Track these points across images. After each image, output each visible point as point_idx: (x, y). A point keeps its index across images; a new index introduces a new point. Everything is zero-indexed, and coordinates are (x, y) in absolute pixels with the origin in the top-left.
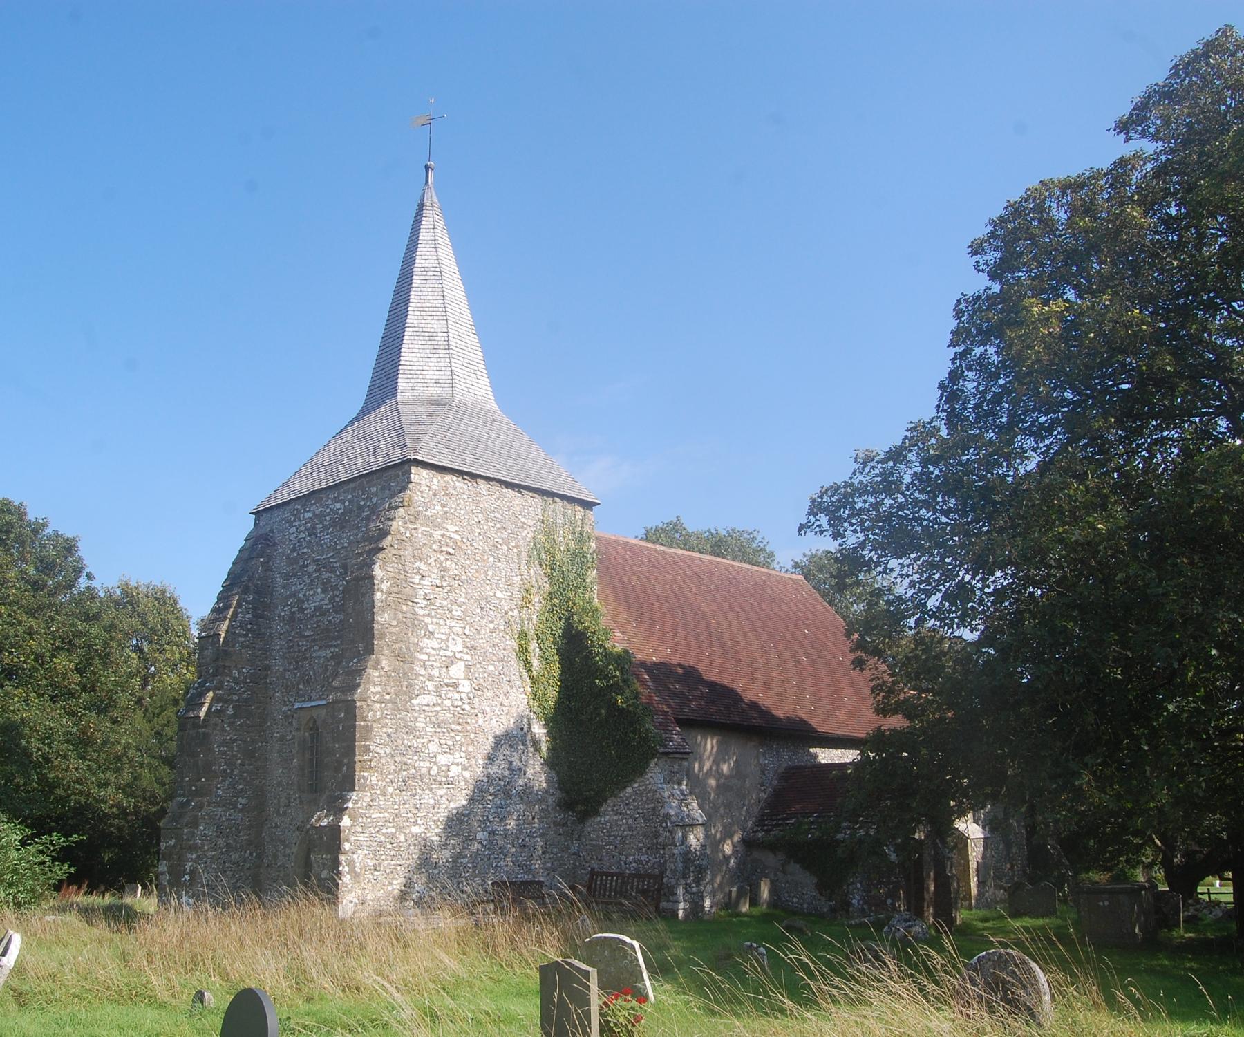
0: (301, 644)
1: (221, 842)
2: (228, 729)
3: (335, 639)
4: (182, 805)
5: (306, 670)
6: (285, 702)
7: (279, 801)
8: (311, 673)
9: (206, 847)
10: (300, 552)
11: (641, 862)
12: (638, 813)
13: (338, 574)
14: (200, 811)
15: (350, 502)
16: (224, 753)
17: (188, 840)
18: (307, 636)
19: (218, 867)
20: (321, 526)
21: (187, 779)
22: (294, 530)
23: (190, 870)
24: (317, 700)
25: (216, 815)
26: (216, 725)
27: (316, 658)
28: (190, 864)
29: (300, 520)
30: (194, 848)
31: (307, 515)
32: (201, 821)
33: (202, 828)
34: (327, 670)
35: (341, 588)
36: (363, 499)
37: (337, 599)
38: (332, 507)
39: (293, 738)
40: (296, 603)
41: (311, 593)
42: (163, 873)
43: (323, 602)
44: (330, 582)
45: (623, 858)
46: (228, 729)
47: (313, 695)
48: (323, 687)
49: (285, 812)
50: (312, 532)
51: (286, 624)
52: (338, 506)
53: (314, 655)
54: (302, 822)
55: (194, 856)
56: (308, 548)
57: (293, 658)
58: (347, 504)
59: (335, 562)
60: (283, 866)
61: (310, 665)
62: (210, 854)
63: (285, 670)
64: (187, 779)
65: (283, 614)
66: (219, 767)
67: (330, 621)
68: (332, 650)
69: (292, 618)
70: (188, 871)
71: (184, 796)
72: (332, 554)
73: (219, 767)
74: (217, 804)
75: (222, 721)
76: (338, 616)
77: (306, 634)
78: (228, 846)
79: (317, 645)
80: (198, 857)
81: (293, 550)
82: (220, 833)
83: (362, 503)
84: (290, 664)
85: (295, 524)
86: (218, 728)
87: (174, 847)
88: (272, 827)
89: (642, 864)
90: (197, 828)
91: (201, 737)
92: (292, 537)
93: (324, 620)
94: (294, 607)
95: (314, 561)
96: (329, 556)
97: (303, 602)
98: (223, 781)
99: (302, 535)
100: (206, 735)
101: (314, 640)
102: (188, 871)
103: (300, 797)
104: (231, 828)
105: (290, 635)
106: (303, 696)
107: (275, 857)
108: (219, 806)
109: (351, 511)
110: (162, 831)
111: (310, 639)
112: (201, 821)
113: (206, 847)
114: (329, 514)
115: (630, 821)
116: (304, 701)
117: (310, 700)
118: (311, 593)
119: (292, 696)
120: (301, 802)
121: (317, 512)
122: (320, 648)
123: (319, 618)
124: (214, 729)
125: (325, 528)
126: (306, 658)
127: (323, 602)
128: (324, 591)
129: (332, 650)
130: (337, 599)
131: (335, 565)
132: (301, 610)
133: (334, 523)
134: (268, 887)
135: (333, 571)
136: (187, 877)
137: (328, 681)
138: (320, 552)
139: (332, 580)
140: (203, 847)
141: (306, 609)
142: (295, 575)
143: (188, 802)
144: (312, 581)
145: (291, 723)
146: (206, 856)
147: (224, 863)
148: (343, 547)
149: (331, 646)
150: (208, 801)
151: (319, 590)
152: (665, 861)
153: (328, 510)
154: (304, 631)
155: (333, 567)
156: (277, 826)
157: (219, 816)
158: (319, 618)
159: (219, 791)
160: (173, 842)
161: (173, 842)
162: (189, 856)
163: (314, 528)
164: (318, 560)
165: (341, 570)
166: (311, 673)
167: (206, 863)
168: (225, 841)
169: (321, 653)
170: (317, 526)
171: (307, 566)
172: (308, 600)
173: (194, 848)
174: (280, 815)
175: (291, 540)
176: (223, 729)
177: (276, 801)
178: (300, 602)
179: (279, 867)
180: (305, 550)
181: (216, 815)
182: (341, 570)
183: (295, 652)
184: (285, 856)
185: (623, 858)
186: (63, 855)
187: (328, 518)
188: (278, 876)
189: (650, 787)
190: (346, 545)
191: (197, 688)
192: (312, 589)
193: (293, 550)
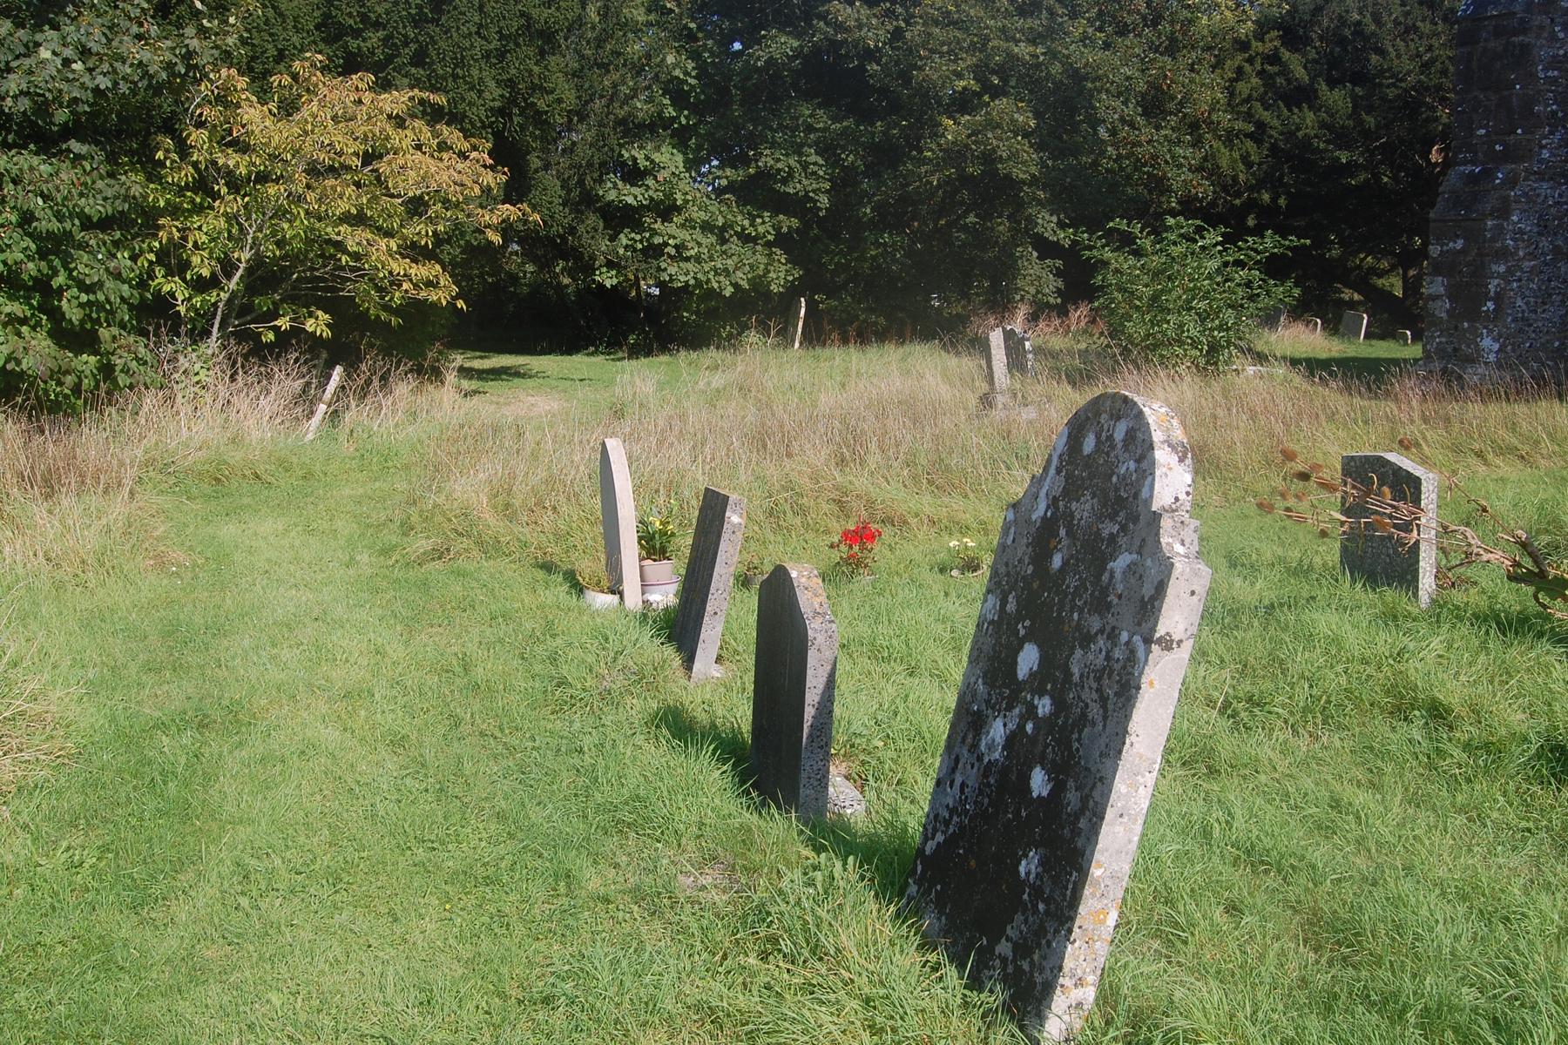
1: (1544, 243)
2: (1561, 35)
4: (1472, 179)
9: (1521, 253)
14: (1512, 189)
16: (1554, 80)
17: (1493, 240)
19: (1540, 289)
21: (1483, 132)
23: (1496, 292)
25: (1538, 195)
26: (1542, 28)
28: (1496, 282)
30: (1503, 254)
32: (1514, 206)
33: (1515, 218)
42: (1434, 298)
46: (1561, 35)
55: (1502, 269)
62: (1527, 265)
64: (1483, 132)
66: (1545, 108)
70: (1492, 294)
71: (1474, 162)
73: (1545, 108)
74: (1541, 176)
75: (1552, 20)
78: (1556, 250)
80: (1509, 271)
82: (1544, 228)
86: (1545, 35)
87: (1463, 251)
90: (1507, 219)
91: (1517, 52)
98: (1552, 133)
100: (1525, 49)
102: (1492, 294)
104: (1560, 219)
108: (1543, 180)
110: (1432, 225)
112: (1514, 206)
113: (1521, 253)
124: (1538, 37)
136: (1490, 305)
140: (1516, 253)
143: (1488, 174)
146: (1521, 270)
147: (1550, 280)
150: (1526, 170)
157: (1542, 198)
159: (1544, 151)
160: (1459, 244)
161: (1459, 244)
162: (1494, 267)
167: (1520, 280)
168: (1551, 242)
173: (1503, 254)
176: (1553, 38)
181: (1538, 195)
186: (1275, 267)
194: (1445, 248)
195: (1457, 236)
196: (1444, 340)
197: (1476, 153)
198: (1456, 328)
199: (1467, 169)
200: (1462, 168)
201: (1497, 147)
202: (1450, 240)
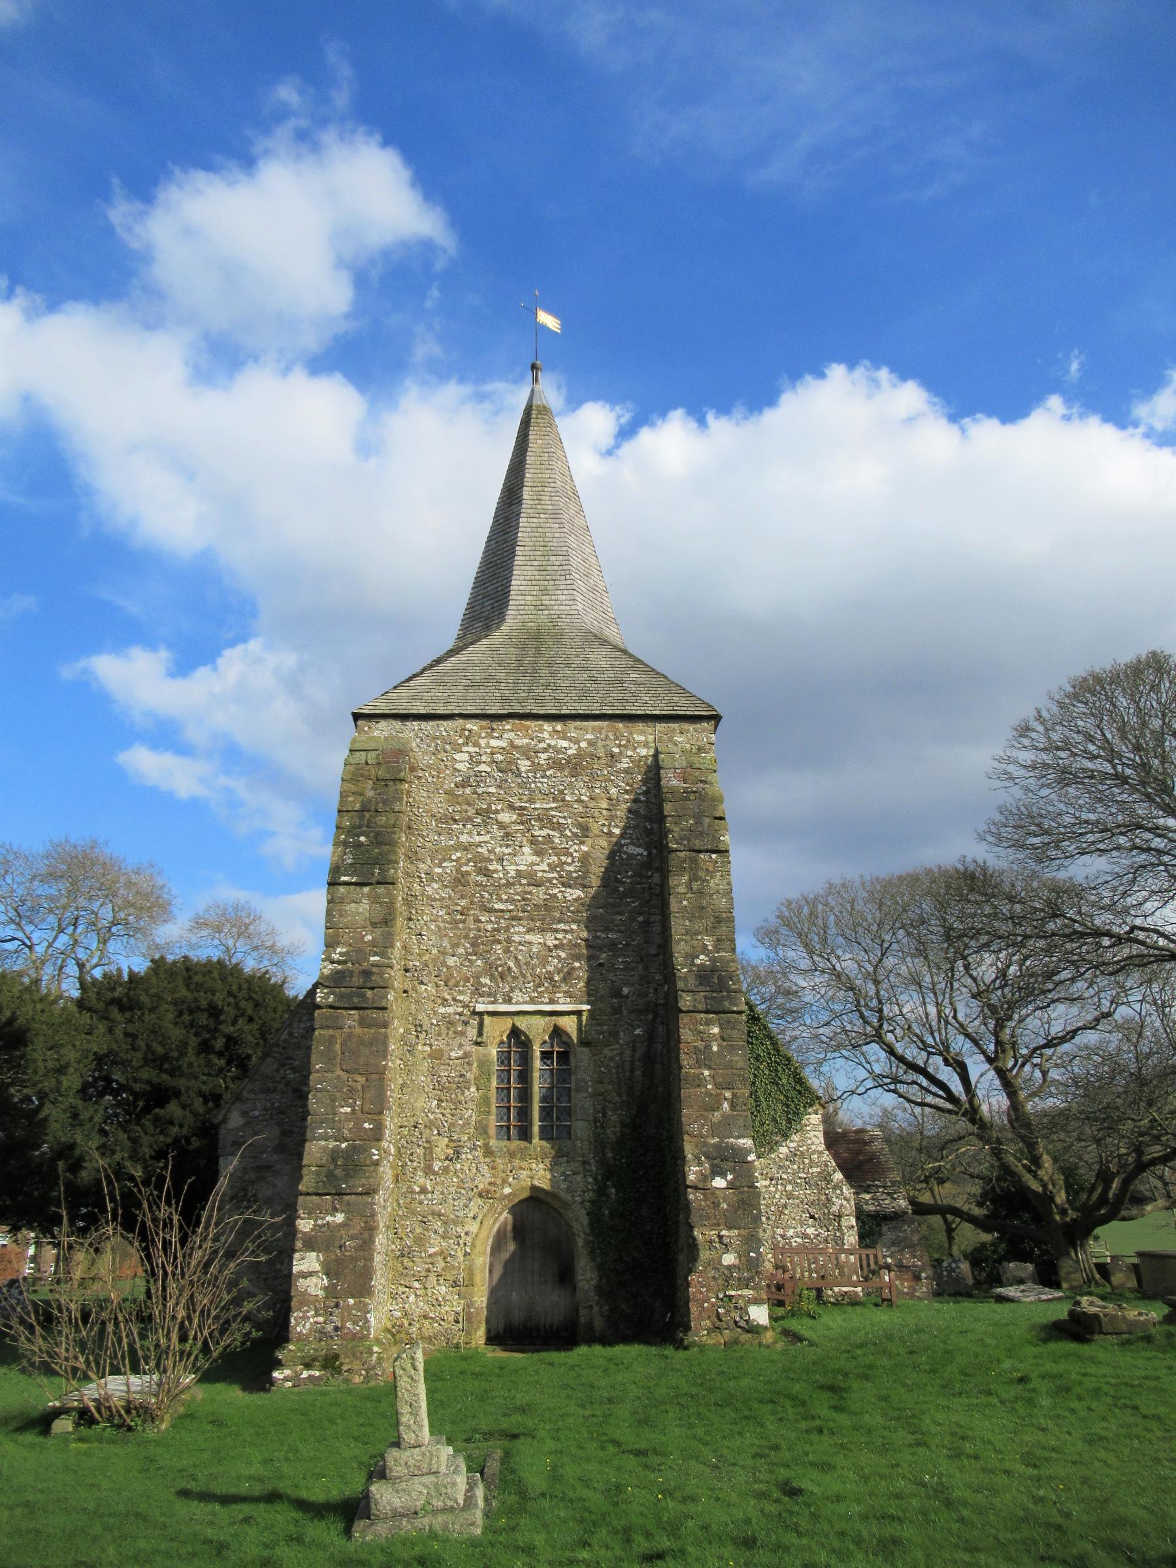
0: (483, 919)
3: (559, 922)
5: (500, 959)
6: (446, 1000)
7: (431, 1153)
8: (511, 964)
10: (479, 791)
11: (805, 1236)
12: (800, 1178)
13: (569, 834)
15: (590, 743)
18: (502, 911)
20: (528, 763)
22: (466, 757)
24: (525, 1003)
27: (520, 943)
29: (476, 744)
31: (494, 743)
34: (544, 962)
35: (575, 854)
36: (619, 746)
37: (567, 868)
38: (553, 743)
39: (466, 1055)
40: (469, 860)
41: (509, 850)
43: (536, 868)
44: (553, 842)
45: (780, 1231)
47: (517, 996)
48: (540, 987)
49: (446, 1170)
50: (507, 767)
51: (446, 886)
52: (565, 744)
53: (516, 938)
54: (490, 1184)
56: (500, 787)
57: (467, 937)
58: (583, 744)
59: (564, 818)
60: (444, 1254)
61: (507, 951)
63: (443, 953)
64: (349, 1110)
65: (439, 870)
67: (554, 896)
68: (560, 936)
69: (460, 880)
72: (554, 805)
76: (572, 891)
77: (498, 906)
79: (521, 925)
81: (464, 784)
83: (616, 750)
84: (457, 945)
85: (465, 749)
87: (343, 1225)
88: (413, 1192)
89: (810, 1239)
92: (458, 766)
93: (540, 894)
94: (467, 865)
95: (511, 807)
96: (545, 806)
97: (491, 861)
99: (483, 767)
101: (513, 919)
103: (486, 1146)
105: (457, 904)
106: (489, 995)
107: (421, 1241)
109: (593, 756)
111: (507, 915)
114: (545, 750)
115: (789, 1187)
116: (493, 1003)
117: (508, 1000)
118: (509, 850)
119: (460, 992)
120: (488, 1152)
121: (518, 742)
122: (529, 930)
123: (528, 889)
125: (535, 767)
126: (499, 942)
127: (536, 868)
128: (539, 853)
129: (560, 936)
130: (567, 868)
131: (562, 821)
132: (487, 873)
133: (555, 764)
134: (402, 1289)
135: (560, 828)
137: (551, 979)
138: (525, 798)
139: (557, 841)
141: (496, 871)
142: (469, 820)
144: (507, 835)
145: (463, 1034)
148: (579, 801)
149: (556, 931)
151: (527, 850)
152: (843, 1234)
153: (542, 745)
154: (489, 901)
155: (558, 823)
156: (423, 1190)
158: (528, 889)
161: (340, 1218)
163: (513, 762)
164: (522, 808)
165: (575, 830)
166: (511, 964)
169: (535, 938)
170: (519, 762)
171: (497, 812)
172: (501, 860)
174: (435, 1173)
175: (459, 771)
177: (420, 1151)
178: (479, 859)
179: (435, 1254)
180: (492, 790)
182: (575, 830)
183: (470, 930)
184: (443, 1237)
185: (780, 1231)
187: (543, 756)
188: (428, 1270)
189: (813, 1147)
190: (583, 798)
191: (339, 962)
192: (507, 846)
193: (464, 784)
194: (320, 1222)
195: (335, 1210)
196: (321, 1319)
197: (339, 1129)
198: (337, 1306)
199: (332, 1144)
200: (323, 1143)
201: (366, 1125)
202: (327, 1214)
